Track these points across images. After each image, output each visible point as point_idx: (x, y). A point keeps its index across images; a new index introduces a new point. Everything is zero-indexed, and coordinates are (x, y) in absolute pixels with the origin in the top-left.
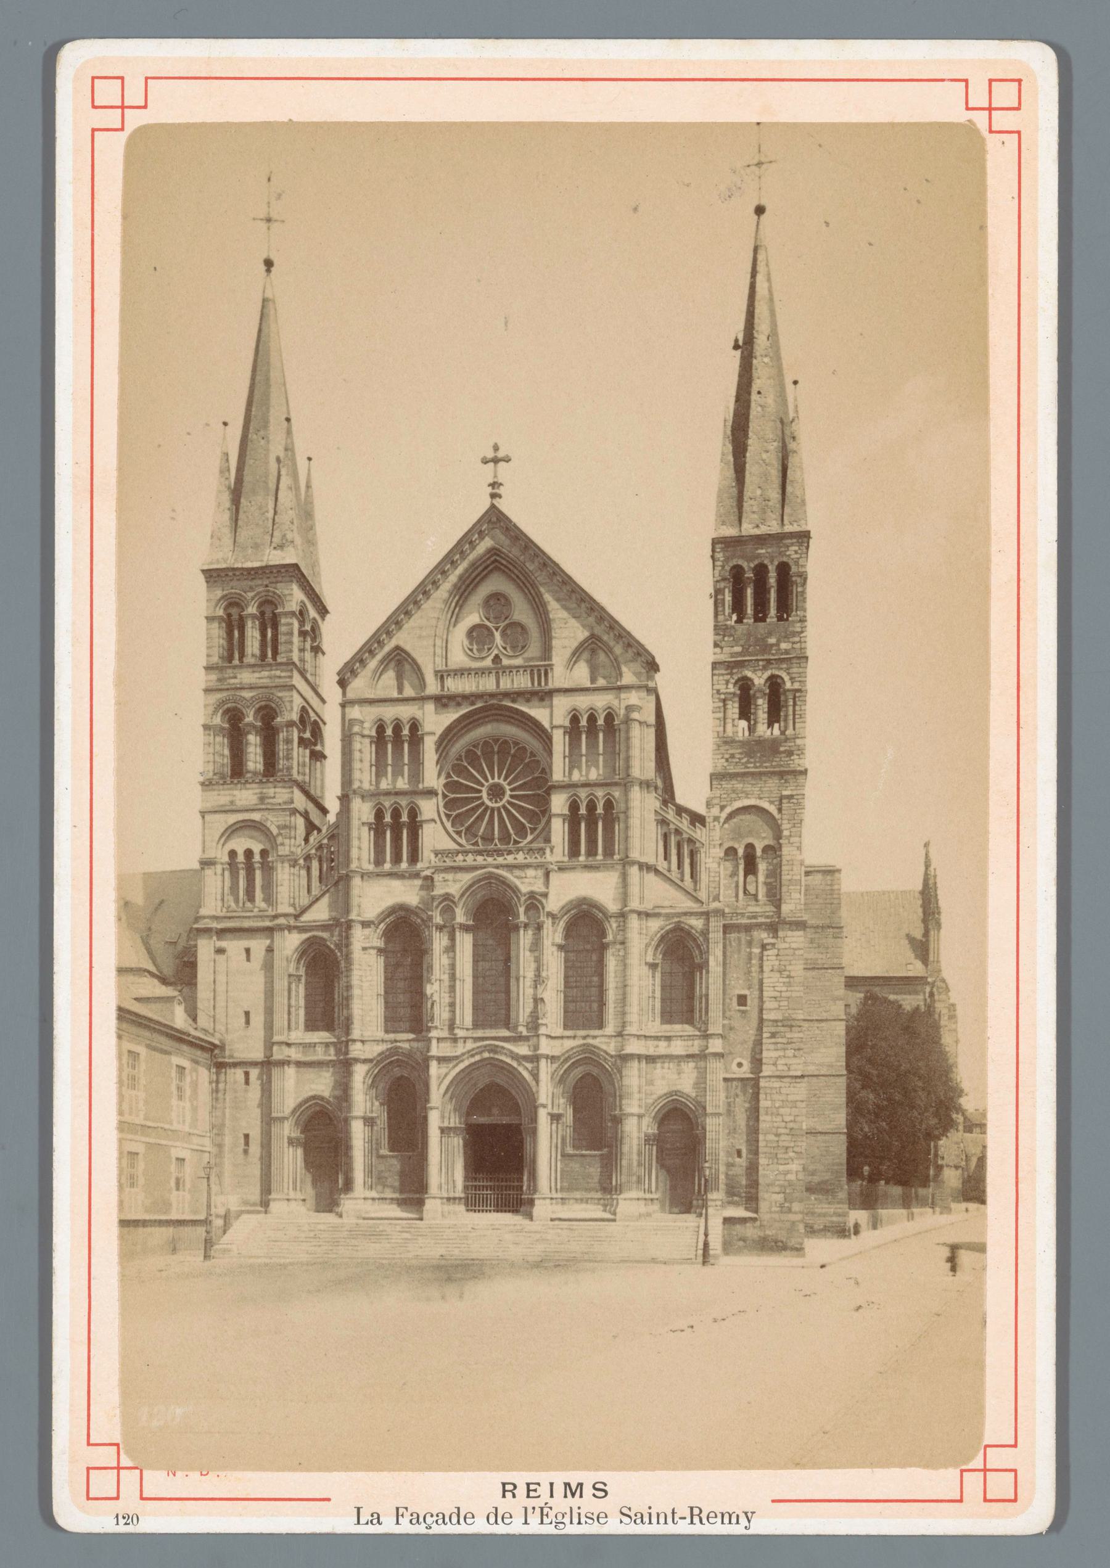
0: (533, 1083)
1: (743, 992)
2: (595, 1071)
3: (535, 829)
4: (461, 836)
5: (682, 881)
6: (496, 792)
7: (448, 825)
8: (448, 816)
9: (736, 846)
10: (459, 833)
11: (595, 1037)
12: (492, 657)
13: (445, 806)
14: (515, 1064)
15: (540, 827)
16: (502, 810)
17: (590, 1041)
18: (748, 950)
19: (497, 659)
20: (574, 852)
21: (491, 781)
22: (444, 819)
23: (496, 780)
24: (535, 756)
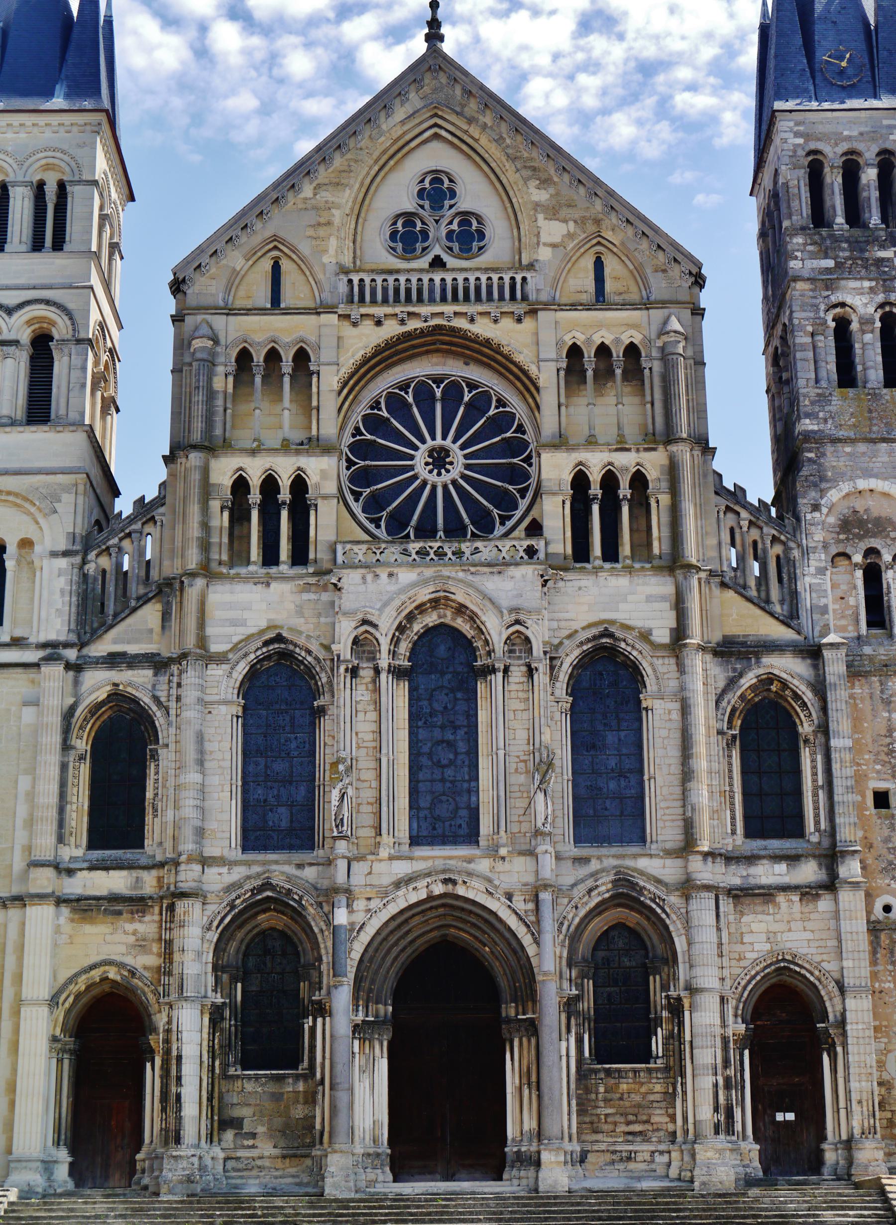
0: (527, 940)
1: (882, 785)
2: (633, 918)
3: (509, 518)
4: (378, 526)
5: (768, 601)
6: (439, 460)
7: (357, 508)
8: (357, 496)
9: (849, 551)
10: (376, 522)
11: (635, 856)
12: (429, 257)
13: (352, 479)
14: (492, 904)
15: (518, 514)
16: (451, 487)
17: (630, 863)
18: (886, 715)
19: (438, 263)
20: (581, 552)
21: (430, 443)
22: (350, 498)
23: (439, 441)
24: (504, 405)
